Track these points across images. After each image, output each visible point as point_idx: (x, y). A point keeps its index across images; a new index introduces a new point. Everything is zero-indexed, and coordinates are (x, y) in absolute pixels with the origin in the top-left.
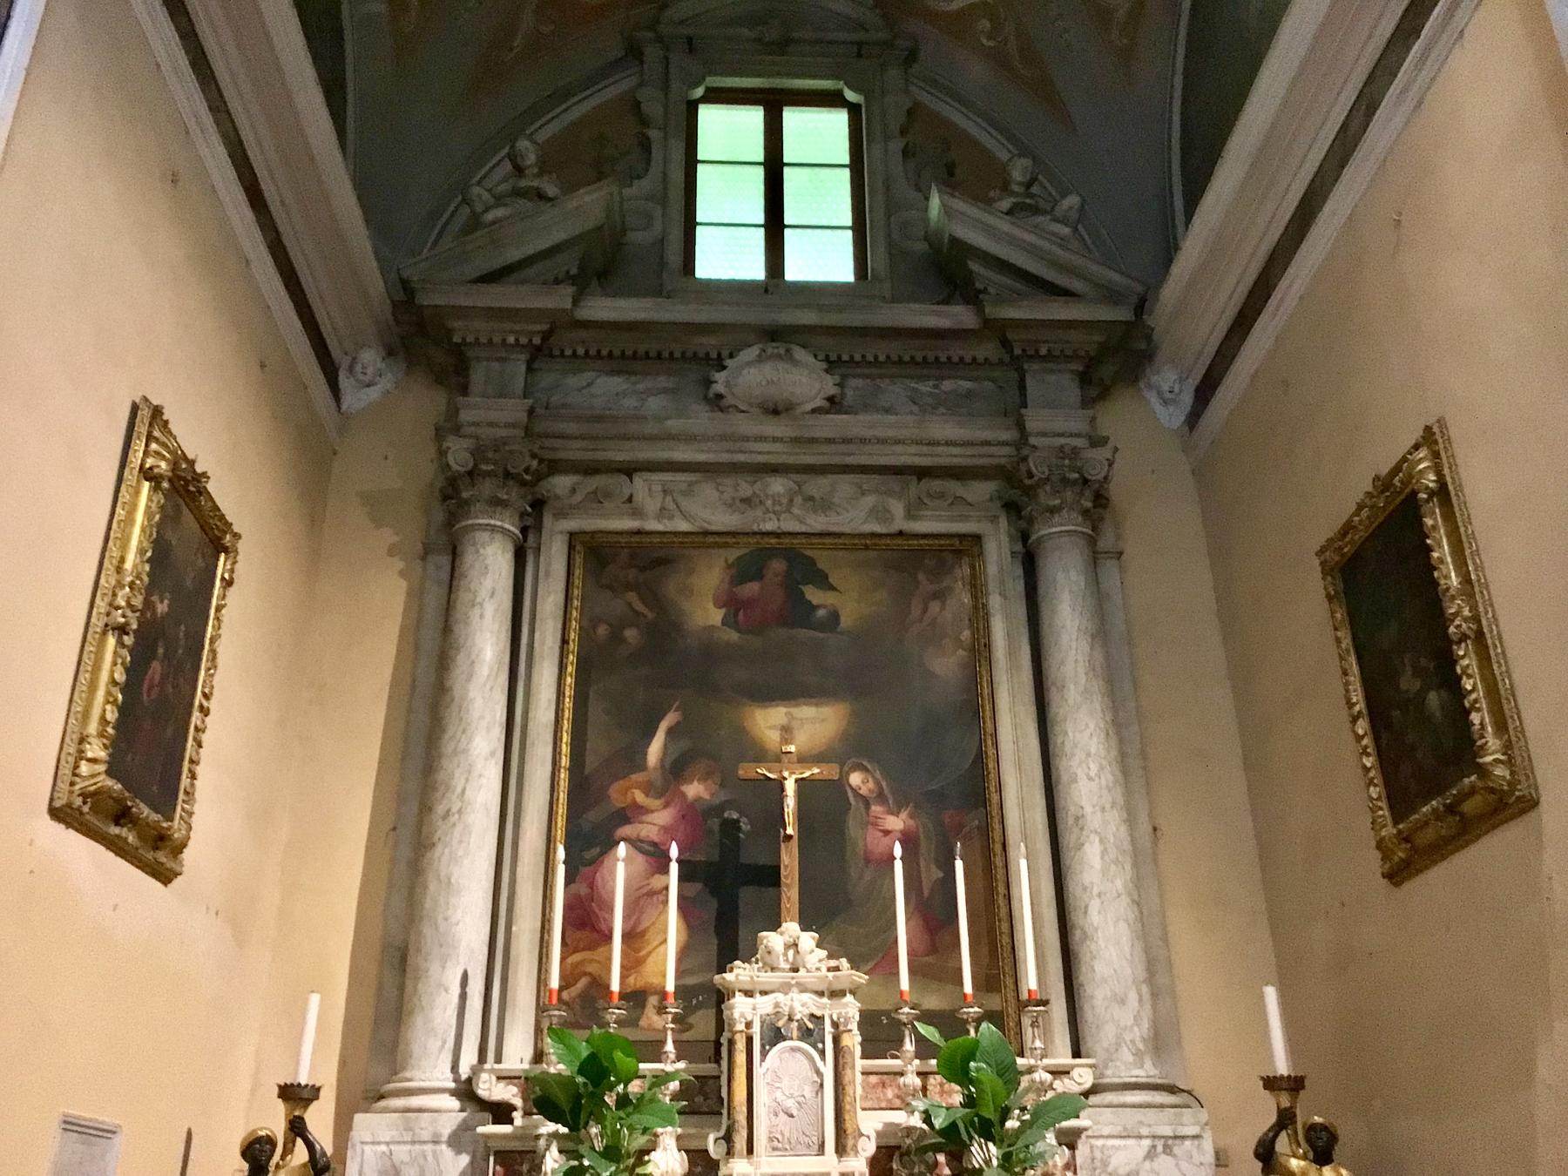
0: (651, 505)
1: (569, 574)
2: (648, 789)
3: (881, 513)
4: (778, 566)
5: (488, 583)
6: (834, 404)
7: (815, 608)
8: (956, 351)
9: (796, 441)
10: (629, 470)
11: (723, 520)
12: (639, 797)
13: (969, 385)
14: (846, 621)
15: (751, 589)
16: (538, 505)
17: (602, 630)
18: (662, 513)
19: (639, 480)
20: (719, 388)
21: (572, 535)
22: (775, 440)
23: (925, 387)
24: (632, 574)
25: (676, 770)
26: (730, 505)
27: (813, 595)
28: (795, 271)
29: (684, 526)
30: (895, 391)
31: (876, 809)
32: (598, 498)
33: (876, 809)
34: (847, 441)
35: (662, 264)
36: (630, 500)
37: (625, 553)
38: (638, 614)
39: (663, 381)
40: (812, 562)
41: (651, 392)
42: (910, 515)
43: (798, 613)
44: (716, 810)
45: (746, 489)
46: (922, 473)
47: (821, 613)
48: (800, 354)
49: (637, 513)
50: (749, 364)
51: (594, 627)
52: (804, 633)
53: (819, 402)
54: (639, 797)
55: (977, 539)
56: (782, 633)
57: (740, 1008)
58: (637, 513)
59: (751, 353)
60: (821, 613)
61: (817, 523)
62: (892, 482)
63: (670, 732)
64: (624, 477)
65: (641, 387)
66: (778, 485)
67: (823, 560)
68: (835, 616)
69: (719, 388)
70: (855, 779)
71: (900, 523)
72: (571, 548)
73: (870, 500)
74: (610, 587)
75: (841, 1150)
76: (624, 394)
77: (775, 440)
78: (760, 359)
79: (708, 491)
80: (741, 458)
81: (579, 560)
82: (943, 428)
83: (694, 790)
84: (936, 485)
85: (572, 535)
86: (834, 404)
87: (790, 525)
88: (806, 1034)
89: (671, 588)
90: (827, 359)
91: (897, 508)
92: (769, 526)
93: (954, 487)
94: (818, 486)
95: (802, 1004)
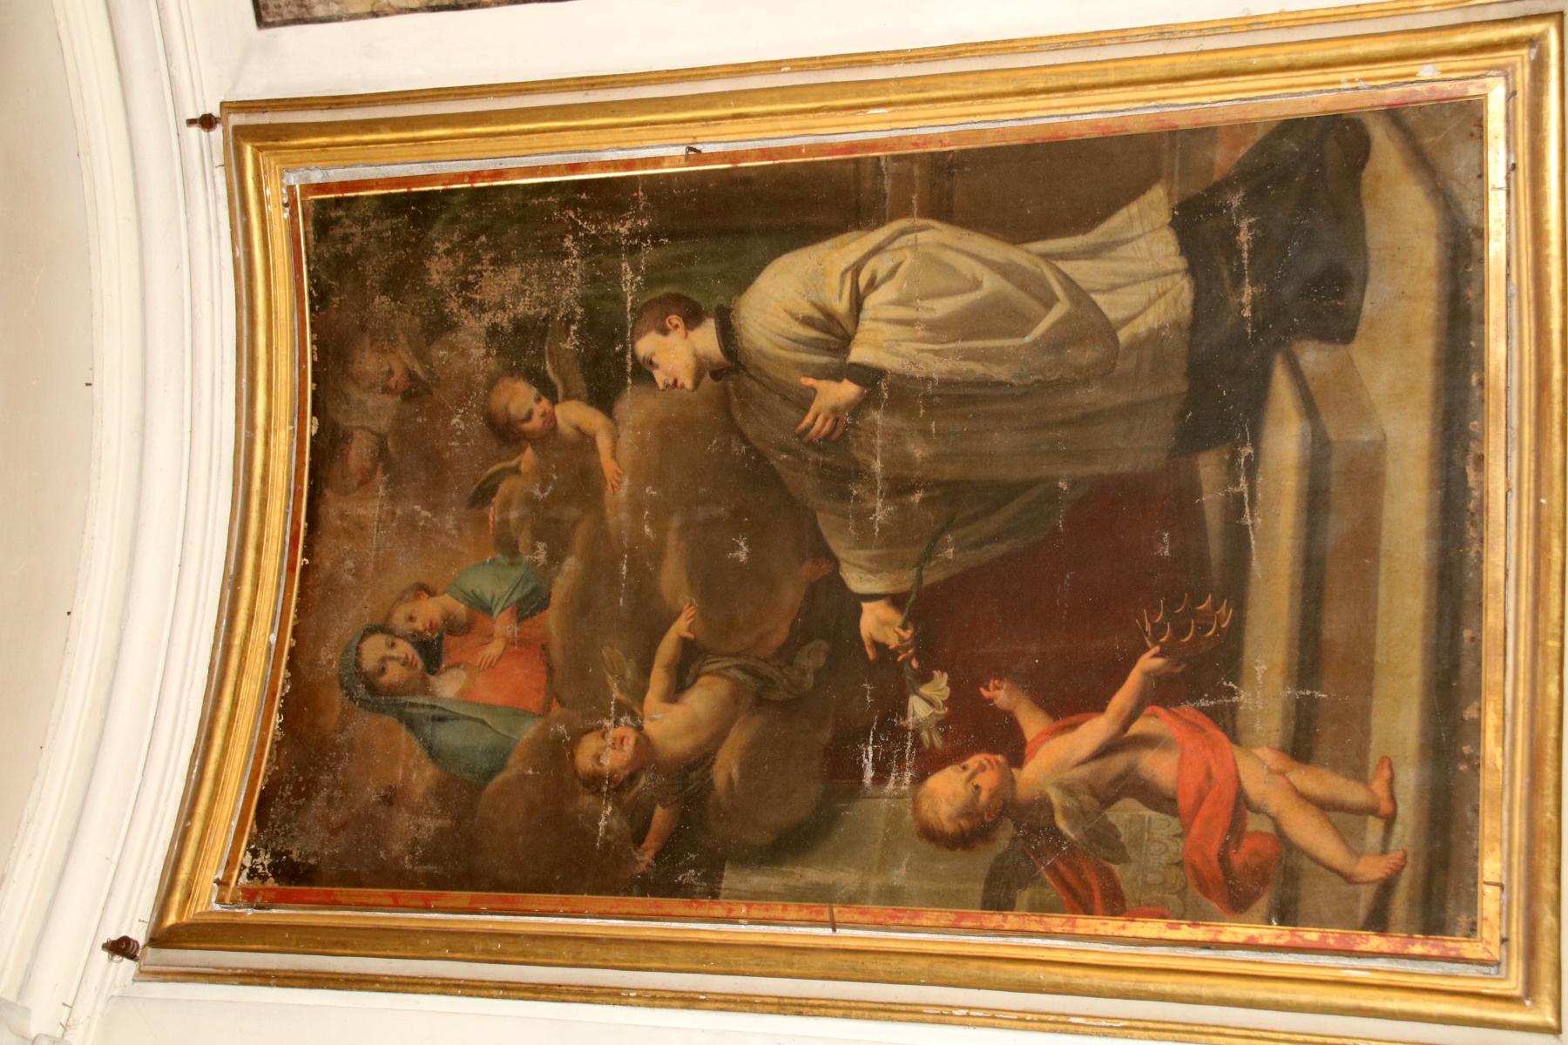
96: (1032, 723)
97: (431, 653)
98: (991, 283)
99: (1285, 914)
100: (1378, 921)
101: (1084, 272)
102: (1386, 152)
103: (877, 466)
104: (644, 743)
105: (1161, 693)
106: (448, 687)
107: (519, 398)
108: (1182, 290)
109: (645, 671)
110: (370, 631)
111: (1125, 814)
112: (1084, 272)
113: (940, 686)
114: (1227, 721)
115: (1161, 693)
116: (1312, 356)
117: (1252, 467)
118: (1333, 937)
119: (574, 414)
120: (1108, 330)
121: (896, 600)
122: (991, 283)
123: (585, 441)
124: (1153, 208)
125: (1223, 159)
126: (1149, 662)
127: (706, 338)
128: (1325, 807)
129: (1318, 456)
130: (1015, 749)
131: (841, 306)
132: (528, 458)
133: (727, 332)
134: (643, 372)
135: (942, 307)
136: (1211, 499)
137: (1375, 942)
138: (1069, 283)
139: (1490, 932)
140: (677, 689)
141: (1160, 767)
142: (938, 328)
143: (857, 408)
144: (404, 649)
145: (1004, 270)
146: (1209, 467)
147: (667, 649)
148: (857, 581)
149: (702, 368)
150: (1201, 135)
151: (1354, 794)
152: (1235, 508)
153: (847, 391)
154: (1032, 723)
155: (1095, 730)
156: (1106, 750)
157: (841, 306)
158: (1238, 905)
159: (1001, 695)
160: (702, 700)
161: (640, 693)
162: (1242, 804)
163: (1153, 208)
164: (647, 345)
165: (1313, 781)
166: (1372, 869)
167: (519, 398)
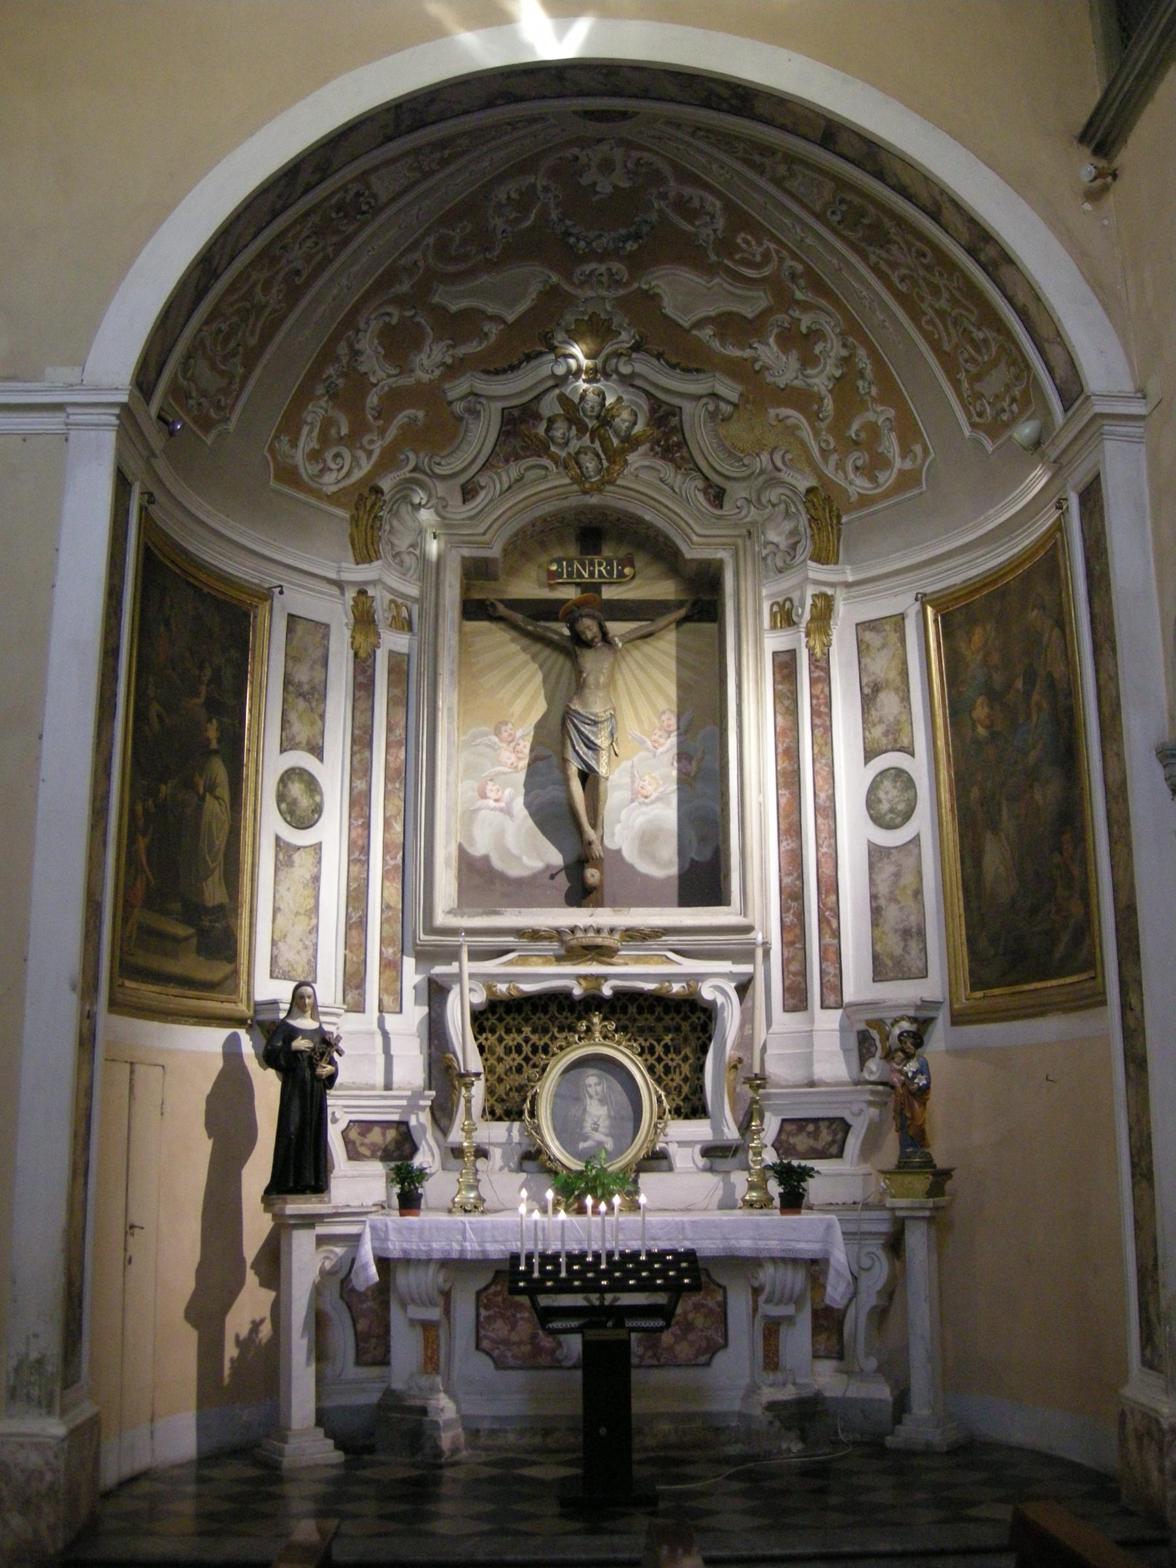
98: (217, 842)
107: (208, 673)
112: (217, 874)
116: (194, 941)
117: (177, 919)
123: (198, 695)
124: (226, 900)
129: (176, 939)
133: (216, 752)
135: (214, 825)
142: (210, 824)
143: (198, 793)
146: (177, 906)
163: (226, 900)
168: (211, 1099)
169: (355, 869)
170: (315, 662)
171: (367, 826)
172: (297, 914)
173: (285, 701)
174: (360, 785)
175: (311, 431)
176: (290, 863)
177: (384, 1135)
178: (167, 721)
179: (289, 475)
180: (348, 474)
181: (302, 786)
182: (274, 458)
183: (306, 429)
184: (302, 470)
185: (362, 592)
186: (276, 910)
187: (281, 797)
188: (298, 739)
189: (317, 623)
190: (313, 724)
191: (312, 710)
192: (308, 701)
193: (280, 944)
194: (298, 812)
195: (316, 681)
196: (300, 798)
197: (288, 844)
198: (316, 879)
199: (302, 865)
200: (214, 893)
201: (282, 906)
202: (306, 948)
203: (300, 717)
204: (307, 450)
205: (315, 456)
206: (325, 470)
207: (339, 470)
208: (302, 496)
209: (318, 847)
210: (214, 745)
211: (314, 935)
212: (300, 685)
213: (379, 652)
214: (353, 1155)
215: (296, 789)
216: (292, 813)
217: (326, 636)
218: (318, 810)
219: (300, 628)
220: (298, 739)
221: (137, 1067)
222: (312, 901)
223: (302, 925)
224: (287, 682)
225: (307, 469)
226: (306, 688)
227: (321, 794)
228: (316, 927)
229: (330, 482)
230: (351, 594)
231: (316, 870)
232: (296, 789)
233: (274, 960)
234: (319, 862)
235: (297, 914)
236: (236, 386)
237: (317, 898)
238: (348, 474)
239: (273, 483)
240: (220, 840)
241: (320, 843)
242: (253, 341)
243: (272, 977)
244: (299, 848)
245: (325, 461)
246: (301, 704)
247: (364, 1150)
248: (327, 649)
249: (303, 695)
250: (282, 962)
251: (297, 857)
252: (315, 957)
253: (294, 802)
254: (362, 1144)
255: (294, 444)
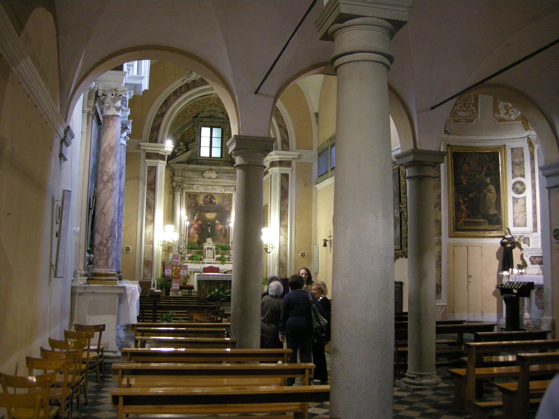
0: (195, 189)
1: (186, 197)
2: (195, 222)
3: (221, 191)
4: (209, 197)
5: (178, 199)
6: (217, 178)
7: (213, 202)
8: (232, 171)
9: (212, 182)
10: (193, 185)
11: (203, 191)
12: (194, 223)
13: (232, 175)
14: (216, 204)
15: (206, 199)
16: (182, 189)
17: (190, 204)
18: (197, 190)
19: (194, 186)
20: (203, 175)
21: (186, 192)
22: (210, 182)
23: (228, 175)
24: (193, 197)
25: (198, 220)
26: (204, 189)
27: (213, 200)
28: (213, 156)
29: (199, 191)
30: (224, 176)
31: (219, 225)
32: (189, 188)
33: (219, 225)
34: (218, 182)
35: (197, 155)
36: (193, 188)
37: (192, 195)
38: (194, 202)
39: (197, 173)
40: (213, 196)
41: (196, 175)
42: (225, 191)
43: (211, 202)
44: (202, 224)
45: (206, 187)
46: (226, 186)
47: (214, 202)
48: (213, 171)
49: (194, 190)
50: (207, 172)
51: (189, 203)
52: (212, 205)
53: (215, 177)
54: (194, 223)
55: (232, 194)
56: (209, 205)
57: (205, 247)
58: (194, 190)
59: (208, 171)
60: (214, 202)
61: (214, 192)
62: (223, 187)
63: (197, 216)
64: (192, 185)
65: (194, 174)
66: (210, 187)
67: (215, 196)
68: (215, 203)
69: (203, 175)
70: (217, 222)
71: (223, 192)
72: (186, 194)
73: (220, 189)
74: (190, 199)
75: (213, 259)
76: (193, 175)
77: (210, 182)
78: (209, 172)
79: (202, 187)
80: (206, 184)
81: (187, 195)
82: (229, 181)
83: (200, 222)
84: (228, 187)
85: (186, 192)
86: (217, 178)
87: (211, 192)
88: (210, 249)
89: (197, 199)
90: (216, 172)
91: (223, 190)
92: (209, 192)
93: (230, 187)
94: (214, 187)
95: (210, 247)
96: (465, 206)
97: (468, 163)
98: (492, 202)
99: (456, 221)
100: (456, 227)
101: (493, 208)
102: (499, 226)
103: (481, 195)
104: (463, 180)
105: (467, 214)
106: (466, 165)
107: (485, 168)
108: (491, 214)
109: (468, 179)
110: (469, 158)
111: (460, 212)
112: (493, 208)
113: (467, 200)
114: (466, 218)
115: (467, 214)
116: (487, 222)
118: (454, 224)
119: (484, 173)
120: (489, 209)
121: (472, 196)
122: (492, 202)
125: (499, 217)
126: (469, 213)
127: (489, 182)
128: (461, 223)
130: (464, 205)
131: (491, 192)
132: (481, 169)
133: (490, 184)
134: (487, 178)
135: (491, 199)
136: (479, 216)
137: (454, 227)
138: (492, 207)
139: (456, 232)
140: (466, 181)
141: (463, 214)
142: (489, 198)
143: (484, 193)
144: (468, 161)
145: (493, 202)
147: (468, 181)
148: (473, 193)
149: (487, 182)
150: (501, 215)
151: (462, 225)
152: (478, 218)
153: (485, 192)
154: (465, 206)
155: (465, 210)
156: (464, 210)
157: (491, 192)
158: (456, 219)
159: (467, 203)
160: (465, 183)
161: (466, 179)
162: (461, 219)
164: (489, 178)
165: (463, 222)
166: (458, 226)
167: (485, 168)
168: (497, 253)
169: (534, 200)
170: (520, 157)
171: (535, 191)
172: (520, 212)
173: (512, 167)
174: (533, 182)
175: (502, 109)
176: (517, 202)
177: (539, 259)
178: (470, 182)
179: (502, 120)
180: (517, 114)
181: (520, 185)
182: (496, 118)
183: (501, 110)
184: (505, 118)
185: (528, 138)
186: (514, 213)
187: (513, 188)
188: (517, 175)
189: (519, 148)
190: (521, 170)
191: (521, 167)
192: (519, 166)
193: (516, 220)
194: (519, 191)
195: (521, 161)
196: (519, 187)
197: (516, 198)
198: (525, 204)
199: (521, 202)
200: (492, 211)
201: (515, 211)
202: (523, 219)
203: (517, 170)
204: (504, 113)
205: (506, 114)
206: (510, 115)
207: (514, 114)
208: (507, 123)
209: (525, 198)
210: (489, 182)
211: (525, 217)
212: (516, 163)
213: (535, 150)
214: (532, 263)
215: (518, 186)
216: (517, 191)
217: (523, 150)
218: (524, 189)
219: (515, 151)
220: (517, 175)
221: (469, 248)
222: (524, 209)
223: (522, 215)
224: (513, 163)
225: (506, 117)
226: (518, 163)
227: (525, 185)
228: (526, 215)
229: (513, 117)
230: (526, 139)
231: (524, 202)
232: (518, 186)
233: (514, 223)
234: (525, 200)
235: (520, 212)
236: (475, 111)
237: (525, 208)
238: (517, 114)
239: (498, 123)
240: (493, 200)
241: (525, 197)
242: (473, 102)
243: (514, 226)
244: (519, 198)
245: (509, 114)
246: (517, 167)
247: (535, 262)
248: (523, 153)
249: (518, 165)
250: (516, 223)
251: (519, 200)
252: (526, 221)
253: (518, 189)
254: (534, 261)
255: (499, 113)
